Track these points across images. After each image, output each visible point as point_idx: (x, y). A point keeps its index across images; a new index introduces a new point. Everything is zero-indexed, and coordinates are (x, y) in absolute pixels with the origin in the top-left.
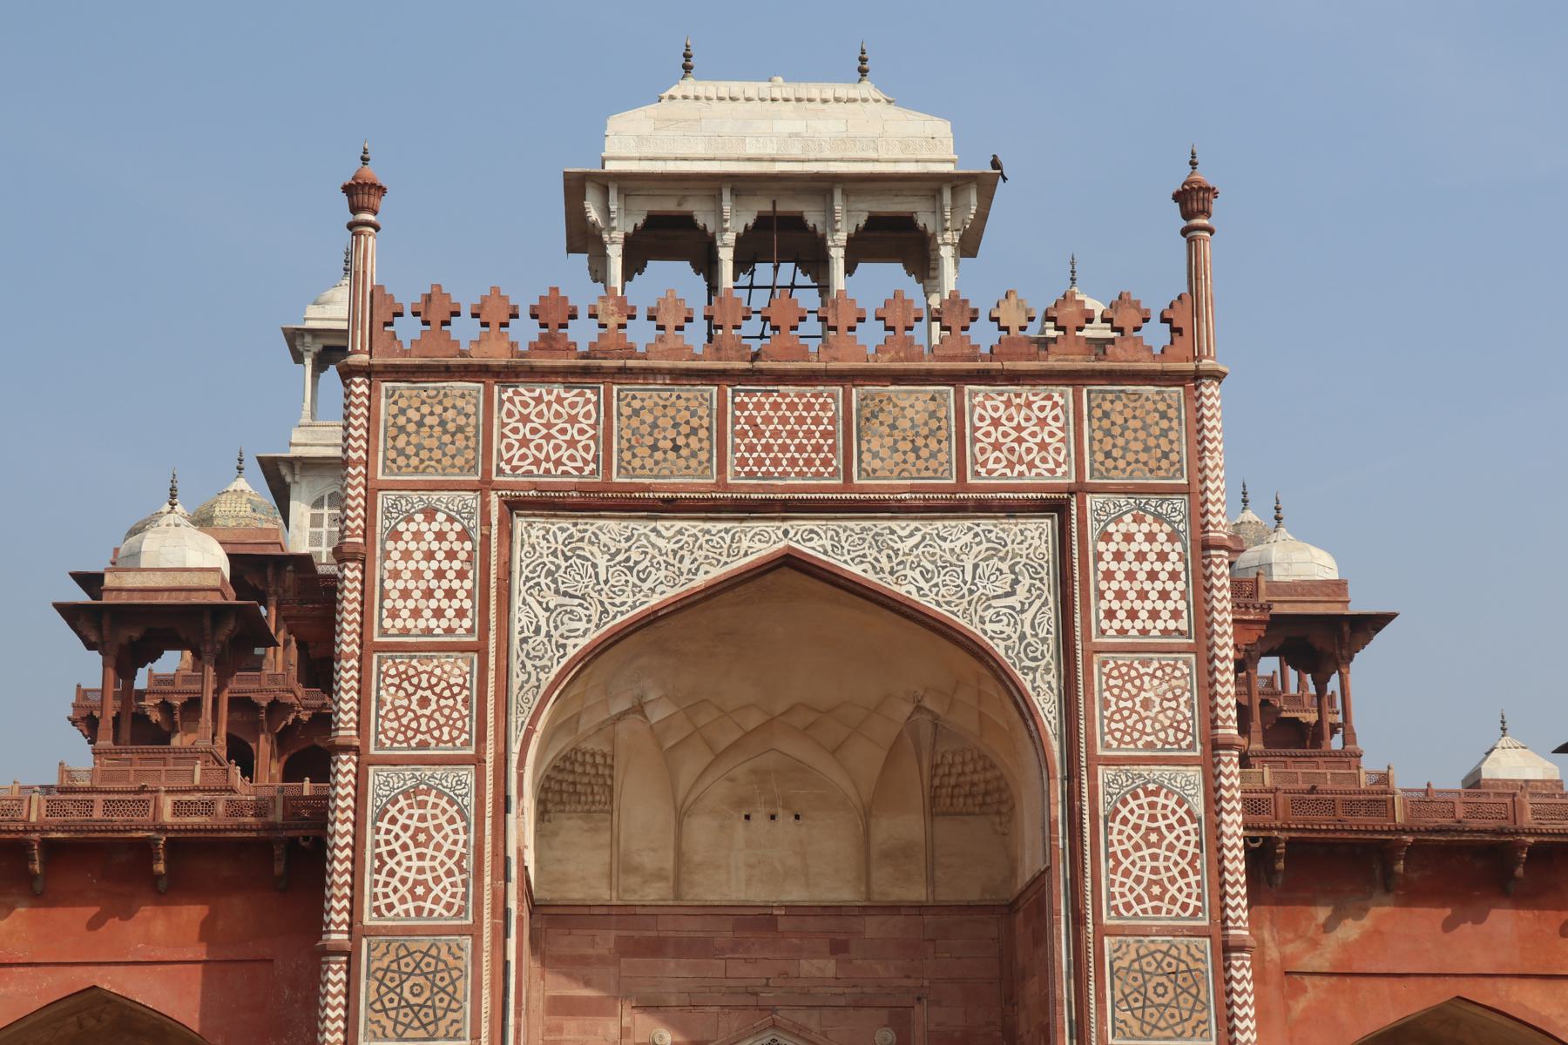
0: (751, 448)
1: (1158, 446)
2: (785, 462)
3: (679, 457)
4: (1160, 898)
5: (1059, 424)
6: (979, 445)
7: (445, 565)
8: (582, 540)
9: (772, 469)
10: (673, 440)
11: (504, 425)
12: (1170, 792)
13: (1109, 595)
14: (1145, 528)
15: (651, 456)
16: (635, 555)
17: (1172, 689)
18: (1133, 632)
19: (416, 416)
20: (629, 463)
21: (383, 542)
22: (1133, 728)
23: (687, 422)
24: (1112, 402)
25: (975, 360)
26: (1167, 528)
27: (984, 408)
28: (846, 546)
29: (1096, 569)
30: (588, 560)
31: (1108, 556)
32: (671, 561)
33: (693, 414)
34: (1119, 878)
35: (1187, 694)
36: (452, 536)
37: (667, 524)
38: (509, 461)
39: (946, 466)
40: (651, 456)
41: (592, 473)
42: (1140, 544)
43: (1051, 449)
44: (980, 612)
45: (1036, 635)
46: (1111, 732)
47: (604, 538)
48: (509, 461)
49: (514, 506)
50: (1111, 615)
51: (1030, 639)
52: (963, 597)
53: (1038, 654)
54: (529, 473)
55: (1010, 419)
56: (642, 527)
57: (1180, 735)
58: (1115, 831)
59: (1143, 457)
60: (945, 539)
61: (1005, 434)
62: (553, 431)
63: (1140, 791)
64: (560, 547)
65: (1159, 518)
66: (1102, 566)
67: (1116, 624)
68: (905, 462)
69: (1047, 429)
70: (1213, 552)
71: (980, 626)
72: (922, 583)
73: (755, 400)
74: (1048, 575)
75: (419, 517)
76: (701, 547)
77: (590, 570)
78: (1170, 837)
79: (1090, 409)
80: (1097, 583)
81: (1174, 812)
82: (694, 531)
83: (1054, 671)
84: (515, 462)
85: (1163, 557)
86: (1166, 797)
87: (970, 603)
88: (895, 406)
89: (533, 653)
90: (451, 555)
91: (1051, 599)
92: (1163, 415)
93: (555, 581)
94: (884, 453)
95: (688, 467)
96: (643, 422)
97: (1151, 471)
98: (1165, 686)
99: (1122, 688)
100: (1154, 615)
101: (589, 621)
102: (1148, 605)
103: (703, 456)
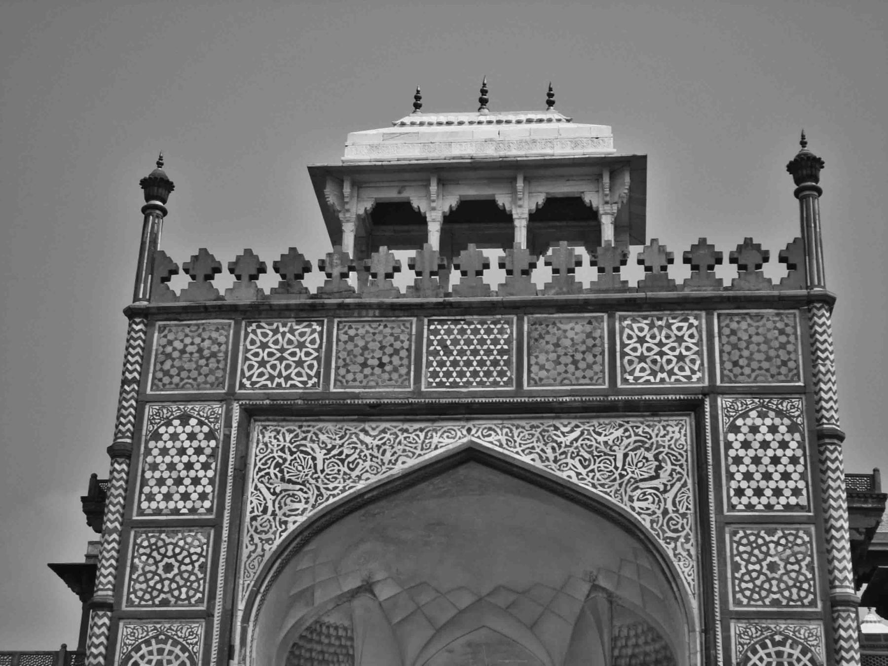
0: (442, 364)
1: (778, 356)
3: (384, 371)
5: (694, 341)
6: (627, 358)
7: (194, 459)
8: (305, 439)
9: (458, 380)
10: (380, 359)
11: (247, 351)
13: (739, 476)
14: (768, 422)
15: (361, 372)
16: (346, 451)
17: (794, 554)
21: (147, 442)
22: (761, 588)
23: (391, 345)
27: (632, 329)
28: (518, 440)
29: (727, 455)
30: (308, 454)
31: (737, 445)
32: (376, 454)
33: (397, 339)
35: (808, 559)
36: (201, 436)
37: (374, 425)
39: (600, 375)
41: (314, 385)
42: (764, 434)
43: (687, 360)
44: (629, 493)
45: (677, 511)
46: (742, 591)
47: (323, 437)
48: (249, 378)
49: (251, 413)
50: (740, 492)
52: (615, 480)
53: (679, 527)
54: (265, 387)
56: (352, 427)
57: (803, 594)
59: (765, 365)
60: (600, 434)
61: (649, 349)
62: (286, 355)
64: (288, 444)
65: (780, 414)
66: (732, 453)
67: (745, 500)
68: (566, 372)
69: (684, 344)
70: (827, 441)
71: (629, 504)
74: (688, 461)
75: (176, 422)
76: (400, 443)
77: (310, 462)
80: (727, 467)
82: (396, 430)
83: (692, 541)
84: (254, 379)
85: (784, 445)
86: (791, 647)
87: (620, 485)
90: (199, 451)
91: (690, 482)
92: (782, 332)
93: (281, 471)
94: (548, 366)
95: (390, 380)
96: (356, 346)
98: (788, 552)
99: (751, 554)
100: (778, 492)
102: (772, 484)
103: (403, 371)
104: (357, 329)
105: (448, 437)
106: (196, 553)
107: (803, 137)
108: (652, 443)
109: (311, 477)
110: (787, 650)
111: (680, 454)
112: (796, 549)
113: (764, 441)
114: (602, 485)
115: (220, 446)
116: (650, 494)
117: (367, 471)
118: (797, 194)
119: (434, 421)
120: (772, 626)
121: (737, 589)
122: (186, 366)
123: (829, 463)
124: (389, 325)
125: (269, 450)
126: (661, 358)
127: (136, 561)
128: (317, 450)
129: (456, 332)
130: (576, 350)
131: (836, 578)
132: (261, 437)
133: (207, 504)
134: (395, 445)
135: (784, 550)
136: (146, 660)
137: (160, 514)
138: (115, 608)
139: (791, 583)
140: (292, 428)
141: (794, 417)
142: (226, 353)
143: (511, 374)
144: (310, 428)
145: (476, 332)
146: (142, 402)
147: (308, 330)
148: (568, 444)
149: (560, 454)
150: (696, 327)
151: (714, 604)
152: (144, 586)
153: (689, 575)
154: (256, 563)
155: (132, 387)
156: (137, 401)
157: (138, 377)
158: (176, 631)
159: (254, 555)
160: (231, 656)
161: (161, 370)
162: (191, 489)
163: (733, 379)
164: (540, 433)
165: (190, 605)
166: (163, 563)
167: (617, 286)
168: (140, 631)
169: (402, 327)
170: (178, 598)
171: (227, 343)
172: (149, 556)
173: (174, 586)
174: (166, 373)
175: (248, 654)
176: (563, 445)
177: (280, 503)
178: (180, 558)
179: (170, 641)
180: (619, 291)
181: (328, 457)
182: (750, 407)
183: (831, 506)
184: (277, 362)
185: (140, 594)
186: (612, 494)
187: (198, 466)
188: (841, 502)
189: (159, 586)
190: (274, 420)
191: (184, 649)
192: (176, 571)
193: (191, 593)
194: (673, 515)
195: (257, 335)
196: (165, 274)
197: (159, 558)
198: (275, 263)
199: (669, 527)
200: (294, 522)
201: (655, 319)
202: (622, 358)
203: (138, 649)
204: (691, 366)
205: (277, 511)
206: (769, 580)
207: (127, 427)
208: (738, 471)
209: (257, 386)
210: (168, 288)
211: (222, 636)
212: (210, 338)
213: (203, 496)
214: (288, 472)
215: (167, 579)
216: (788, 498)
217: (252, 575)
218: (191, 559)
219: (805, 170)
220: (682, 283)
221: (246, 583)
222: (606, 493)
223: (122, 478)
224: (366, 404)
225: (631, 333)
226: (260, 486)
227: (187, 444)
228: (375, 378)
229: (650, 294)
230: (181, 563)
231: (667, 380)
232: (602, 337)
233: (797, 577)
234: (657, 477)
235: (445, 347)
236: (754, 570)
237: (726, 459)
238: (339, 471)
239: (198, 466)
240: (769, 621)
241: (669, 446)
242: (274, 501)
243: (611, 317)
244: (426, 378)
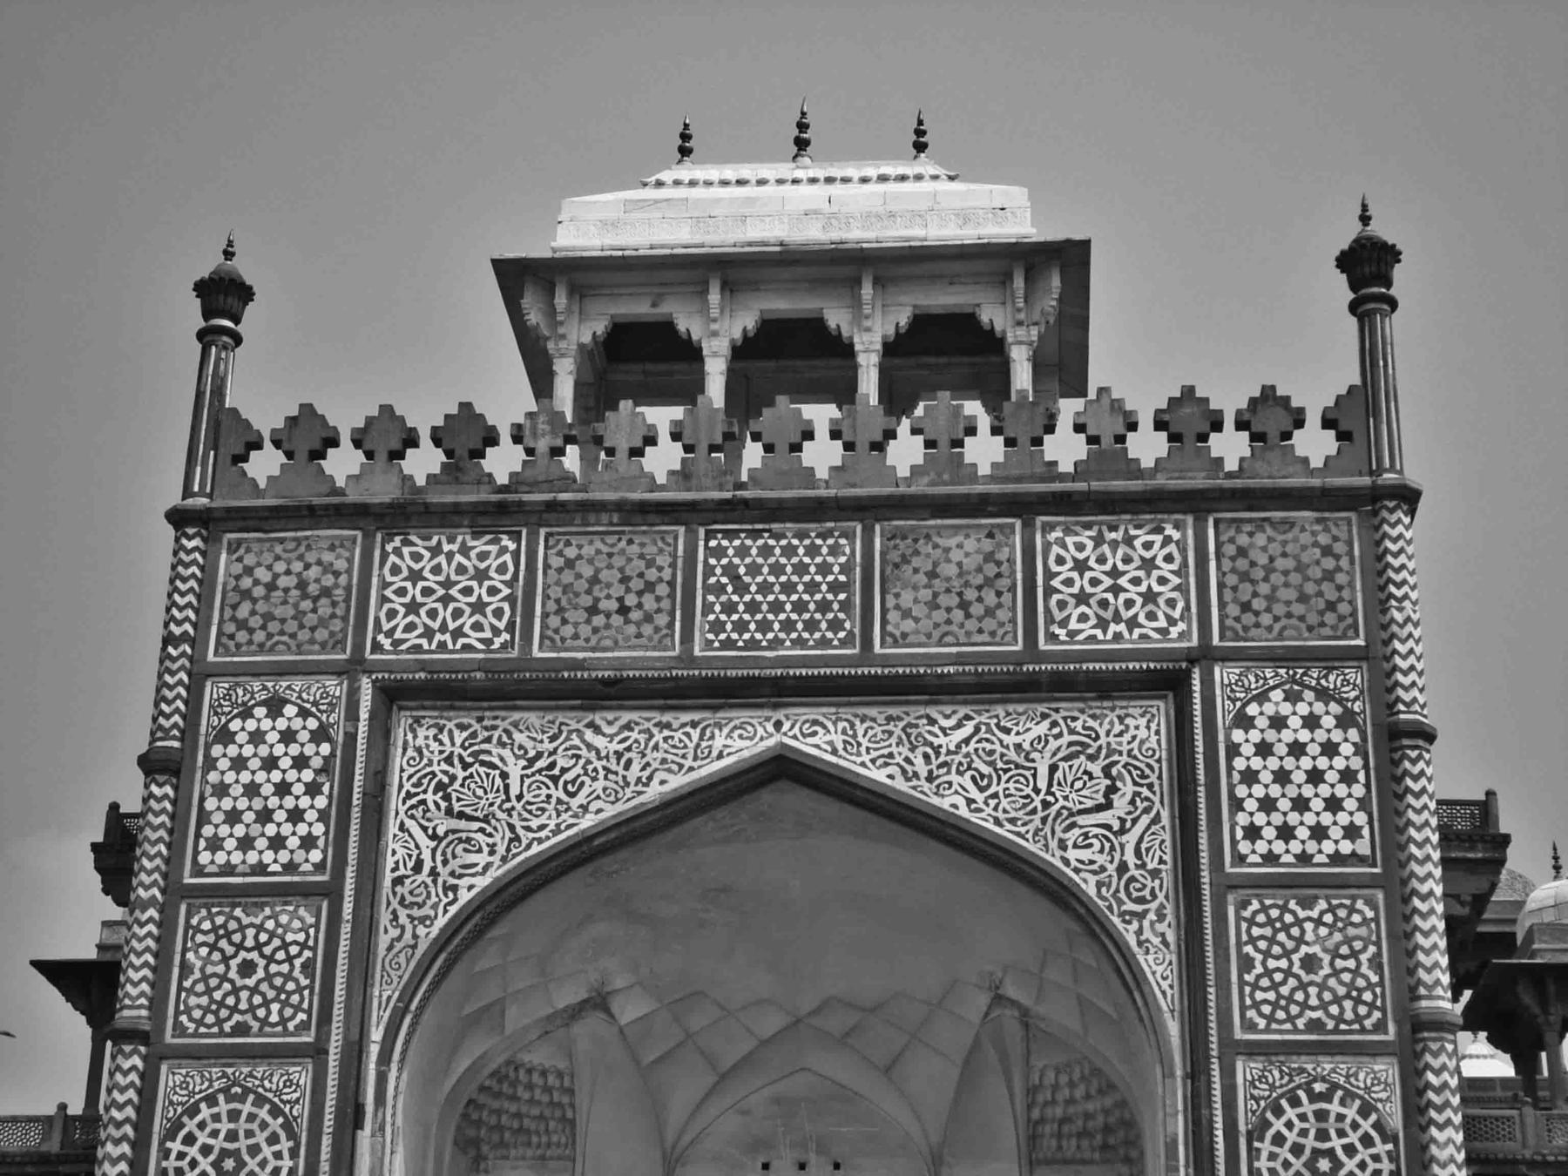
0: (730, 608)
1: (1320, 594)
3: (627, 621)
6: (1056, 597)
7: (292, 776)
8: (488, 740)
9: (758, 636)
10: (620, 600)
11: (385, 585)
12: (1348, 1097)
15: (588, 621)
16: (561, 763)
17: (1348, 941)
20: (556, 631)
21: (208, 747)
23: (641, 575)
24: (1251, 534)
29: (1230, 768)
30: (495, 767)
31: (1247, 750)
32: (614, 767)
33: (650, 563)
35: (1372, 949)
36: (304, 736)
37: (610, 716)
38: (390, 633)
39: (1009, 627)
41: (504, 646)
43: (1161, 601)
44: (1059, 834)
45: (1143, 866)
46: (1256, 1005)
47: (519, 738)
48: (390, 633)
49: (393, 695)
50: (1253, 833)
51: (1133, 872)
52: (1034, 811)
53: (1146, 893)
54: (417, 649)
55: (1102, 560)
56: (572, 720)
57: (1362, 1010)
58: (1264, 1155)
59: (1298, 609)
60: (1007, 731)
61: (1095, 582)
62: (454, 592)
63: (1301, 1093)
64: (457, 750)
65: (1323, 695)
66: (1239, 764)
67: (1261, 846)
68: (949, 622)
69: (1155, 573)
70: (1406, 742)
71: (1058, 853)
74: (1162, 776)
75: (260, 712)
77: (498, 781)
80: (1231, 788)
81: (1355, 1126)
82: (647, 725)
83: (1170, 918)
84: (398, 635)
85: (1330, 749)
86: (1342, 1103)
87: (1044, 820)
90: (300, 762)
91: (1165, 814)
92: (1327, 551)
93: (447, 798)
95: (639, 636)
96: (579, 576)
98: (1338, 937)
99: (1272, 941)
100: (1319, 833)
102: (1310, 819)
103: (662, 620)
104: (580, 547)
105: (741, 737)
106: (296, 943)
107: (1364, 207)
108: (1100, 748)
109: (500, 807)
110: (1334, 1107)
111: (1148, 765)
112: (1351, 931)
113: (1296, 742)
114: (1013, 821)
115: (339, 753)
116: (1096, 836)
117: (598, 797)
118: (1353, 308)
119: (715, 708)
120: (1309, 1067)
121: (1248, 1002)
122: (278, 612)
123: (1409, 782)
125: (425, 761)
126: (1116, 598)
127: (190, 956)
128: (510, 759)
129: (754, 551)
130: (967, 584)
131: (1419, 982)
132: (410, 736)
133: (316, 856)
134: (648, 751)
135: (1331, 934)
136: (208, 1130)
137: (232, 874)
139: (1342, 991)
140: (465, 721)
141: (1347, 700)
142: (348, 589)
143: (852, 625)
144: (498, 722)
145: (789, 551)
146: (199, 676)
147: (493, 548)
148: (952, 748)
149: (939, 767)
150: (1177, 543)
151: (1207, 1028)
152: (204, 1000)
153: (1164, 979)
154: (402, 959)
155: (181, 649)
156: (190, 675)
157: (191, 631)
158: (262, 1080)
159: (398, 946)
160: (358, 1124)
161: (233, 619)
162: (287, 829)
163: (1241, 633)
164: (904, 729)
165: (286, 1033)
166: (239, 960)
167: (1039, 470)
168: (198, 1079)
169: (660, 544)
170: (264, 1022)
171: (349, 571)
172: (213, 947)
173: (257, 1000)
174: (242, 625)
175: (389, 1119)
176: (943, 750)
177: (444, 854)
178: (267, 950)
179: (251, 1097)
180: (1043, 480)
181: (529, 772)
182: (1271, 682)
183: (1411, 857)
184: (439, 605)
185: (197, 1014)
186: (1029, 836)
187: (298, 789)
188: (1429, 849)
189: (230, 1001)
190: (434, 708)
191: (275, 1112)
192: (260, 973)
193: (288, 1012)
194: (1136, 873)
195: (401, 556)
196: (239, 450)
197: (230, 950)
198: (434, 429)
199: (1129, 895)
200: (470, 888)
201: (1104, 528)
203: (193, 1111)
204: (1169, 611)
206: (1303, 986)
207: (172, 720)
208: (1250, 795)
209: (404, 647)
210: (244, 474)
211: (342, 1087)
212: (319, 563)
213: (308, 842)
214: (459, 800)
215: (245, 987)
216: (1336, 842)
217: (396, 980)
218: (287, 953)
219: (1368, 265)
220: (1152, 465)
221: (385, 995)
222: (1018, 834)
223: (164, 811)
224: (597, 678)
225: (1062, 552)
226: (409, 823)
227: (279, 750)
228: (613, 632)
229: (1096, 485)
230: (270, 959)
231: (1126, 635)
232: (1011, 561)
233: (1353, 981)
234: (1108, 805)
235: (735, 578)
236: (1278, 969)
237: (1229, 775)
238: (549, 796)
239: (298, 789)
240: (1303, 1058)
241: (1130, 752)
242: (434, 851)
243: (1028, 526)
244: (703, 634)
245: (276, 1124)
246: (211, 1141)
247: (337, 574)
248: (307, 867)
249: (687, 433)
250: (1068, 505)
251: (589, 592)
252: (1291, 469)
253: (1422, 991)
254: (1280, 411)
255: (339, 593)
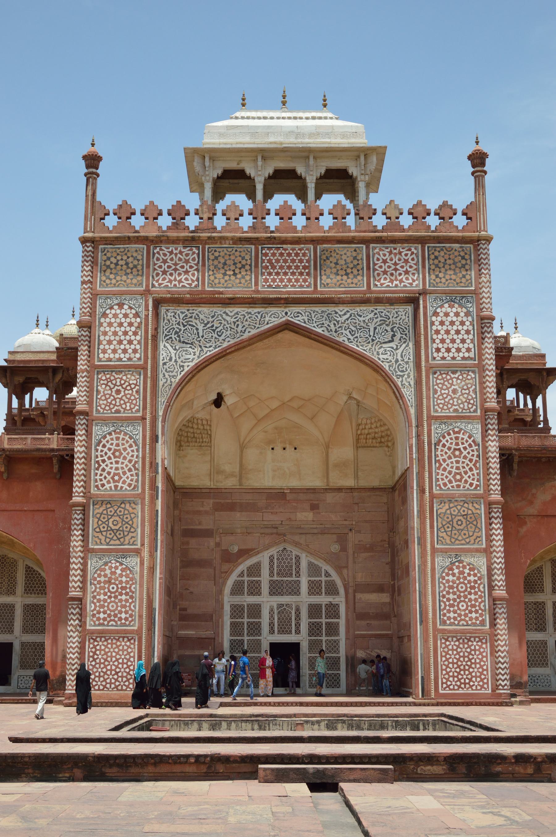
2: (286, 280)
4: (460, 481)
5: (414, 262)
6: (376, 272)
7: (128, 329)
8: (191, 317)
9: (280, 284)
11: (155, 264)
13: (437, 341)
14: (454, 310)
15: (223, 278)
17: (466, 384)
18: (449, 358)
19: (114, 261)
20: (213, 281)
21: (99, 319)
22: (448, 403)
23: (240, 262)
24: (439, 252)
25: (375, 232)
26: (464, 310)
28: (315, 319)
31: (437, 323)
32: (233, 327)
34: (441, 472)
35: (474, 387)
36: (131, 316)
37: (231, 309)
38: (157, 281)
40: (223, 278)
41: (196, 286)
46: (438, 404)
47: (202, 317)
50: (438, 350)
58: (439, 450)
60: (361, 316)
61: (389, 267)
62: (178, 267)
64: (181, 321)
66: (434, 328)
67: (441, 355)
69: (409, 264)
70: (486, 321)
71: (377, 356)
72: (350, 336)
73: (272, 251)
75: (116, 307)
77: (195, 331)
78: (465, 453)
79: (429, 255)
81: (467, 441)
83: (412, 377)
84: (160, 282)
85: (462, 323)
86: (463, 434)
88: (337, 254)
89: (168, 370)
90: (131, 324)
92: (463, 258)
93: (179, 336)
96: (219, 262)
97: (457, 284)
98: (463, 383)
99: (443, 384)
100: (458, 350)
101: (194, 355)
102: (456, 346)
124: (238, 250)
127: (99, 388)
130: (348, 267)
133: (138, 355)
137: (111, 361)
138: (90, 414)
140: (183, 311)
142: (143, 265)
147: (190, 252)
154: (167, 389)
162: (128, 347)
166: (115, 389)
167: (371, 228)
170: (125, 409)
171: (142, 259)
172: (107, 385)
173: (122, 402)
178: (124, 386)
184: (173, 272)
185: (103, 406)
187: (130, 333)
189: (114, 402)
191: (131, 438)
193: (132, 406)
194: (401, 363)
195: (159, 254)
197: (112, 386)
198: (169, 210)
200: (188, 366)
202: (374, 272)
203: (105, 437)
205: (178, 360)
212: (132, 256)
213: (135, 351)
226: (167, 345)
228: (231, 282)
232: (362, 259)
237: (431, 332)
239: (130, 333)
242: (175, 354)
245: (131, 441)
246: (111, 447)
247: (138, 260)
248: (135, 359)
249: (254, 213)
250: (380, 240)
251: (223, 268)
252: (452, 230)
253: (488, 400)
254: (449, 209)
255: (139, 267)
